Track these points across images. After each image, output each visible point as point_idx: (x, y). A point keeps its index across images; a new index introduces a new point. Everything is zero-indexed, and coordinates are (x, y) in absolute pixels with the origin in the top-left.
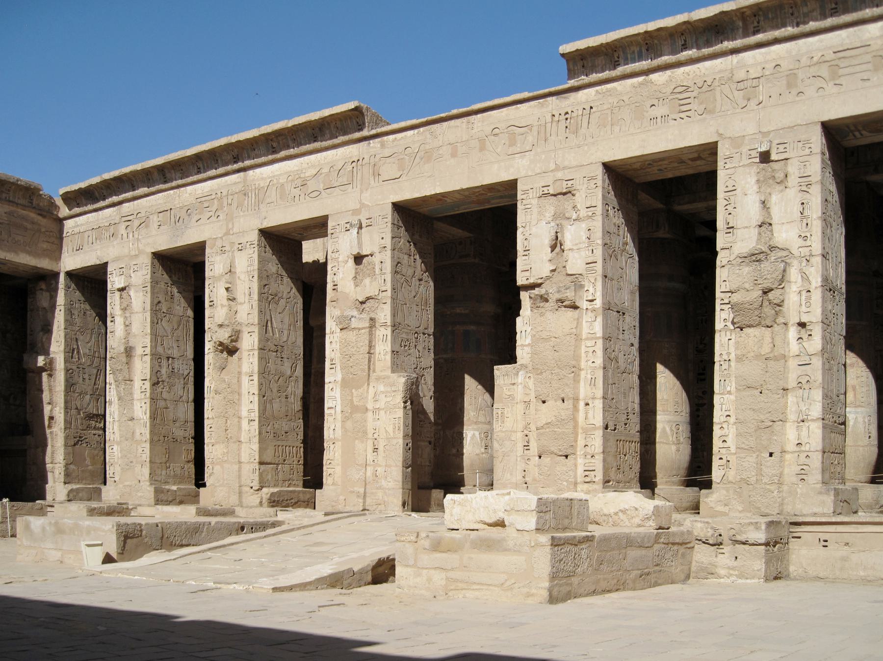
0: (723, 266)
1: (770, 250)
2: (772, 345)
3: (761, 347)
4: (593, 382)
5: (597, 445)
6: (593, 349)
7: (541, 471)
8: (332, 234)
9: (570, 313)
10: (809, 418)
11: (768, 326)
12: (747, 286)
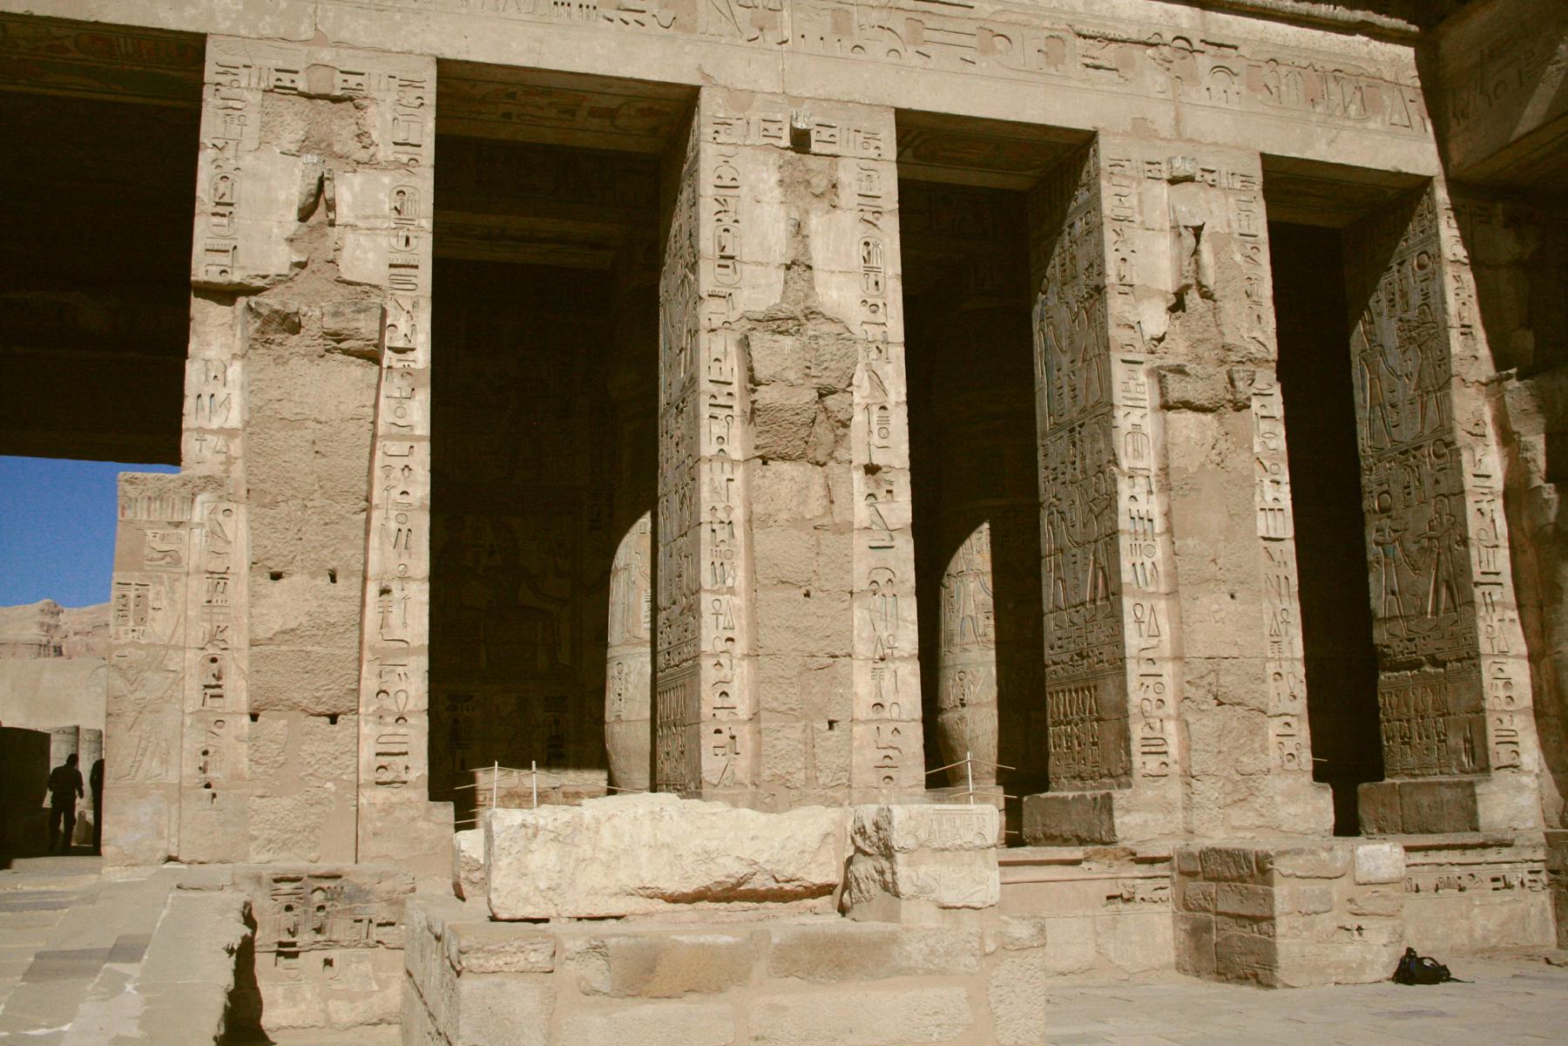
0: (713, 330)
1: (806, 316)
2: (825, 502)
3: (804, 502)
4: (402, 540)
5: (412, 692)
6: (406, 461)
7: (258, 755)
9: (358, 371)
10: (896, 654)
11: (817, 463)
12: (791, 375)
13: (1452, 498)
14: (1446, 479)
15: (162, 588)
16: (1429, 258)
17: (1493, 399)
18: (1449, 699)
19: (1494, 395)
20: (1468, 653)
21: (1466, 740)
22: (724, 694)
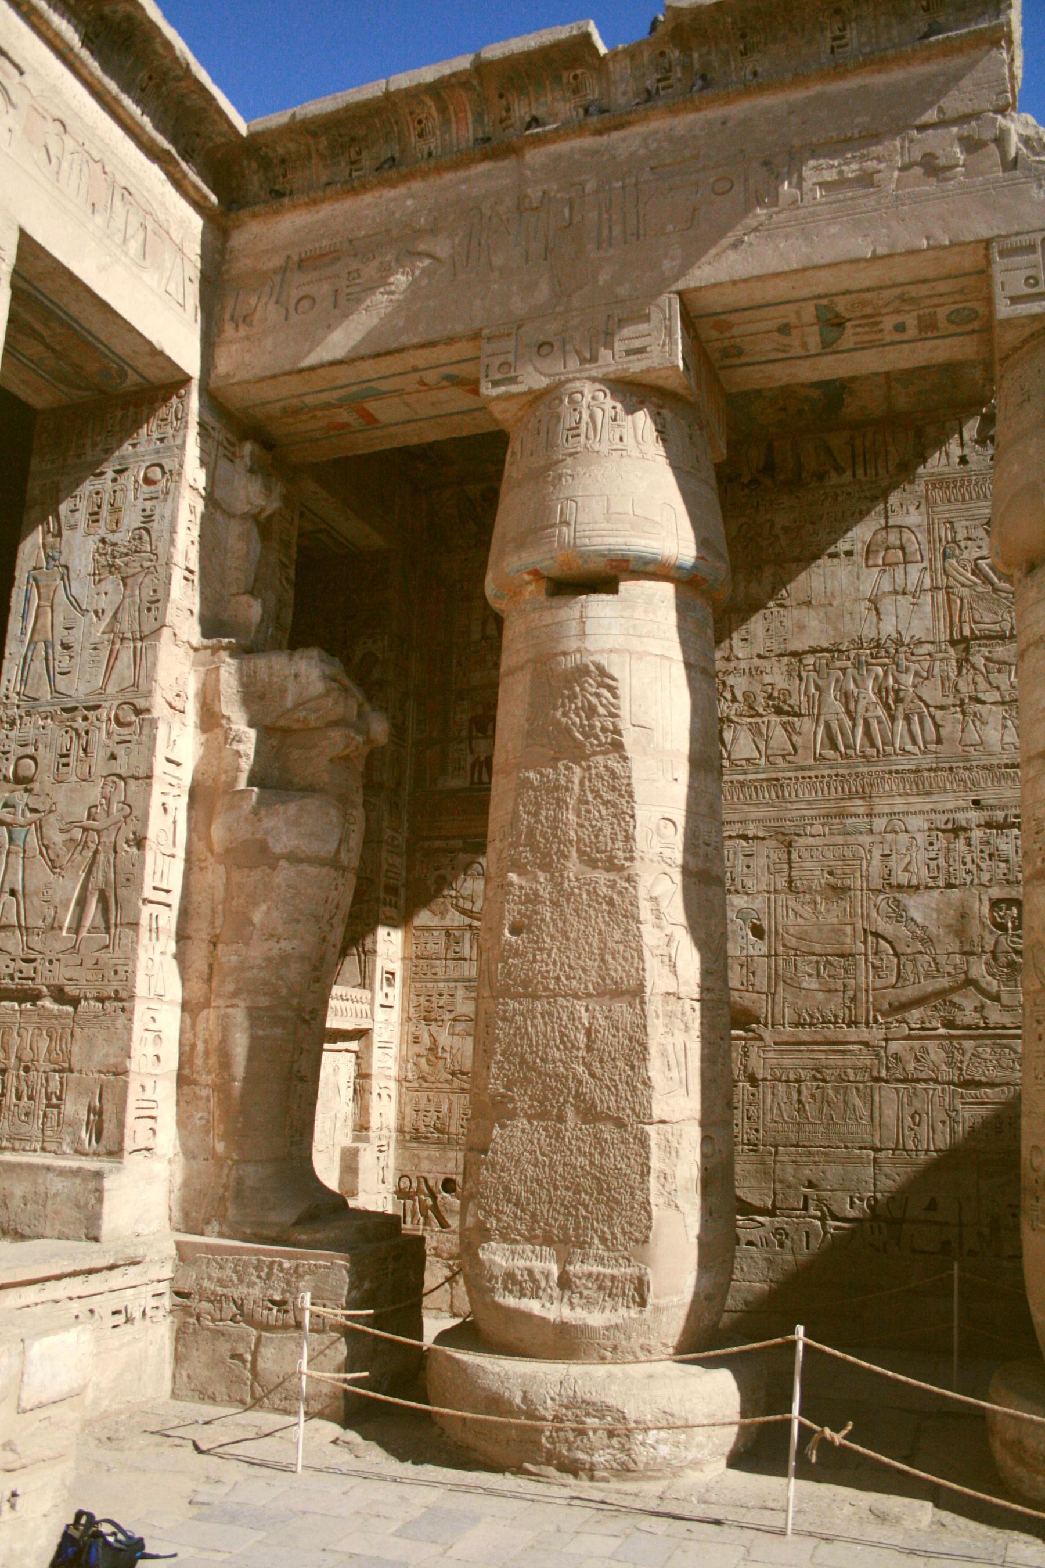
13: (131, 781)
14: (128, 755)
16: (164, 473)
17: (202, 669)
18: (75, 1049)
19: (204, 665)
20: (116, 992)
21: (90, 1110)
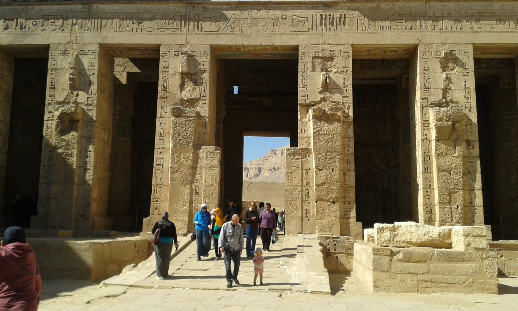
5: (351, 197)
7: (318, 210)
8: (163, 56)
15: (296, 173)
22: (429, 199)
